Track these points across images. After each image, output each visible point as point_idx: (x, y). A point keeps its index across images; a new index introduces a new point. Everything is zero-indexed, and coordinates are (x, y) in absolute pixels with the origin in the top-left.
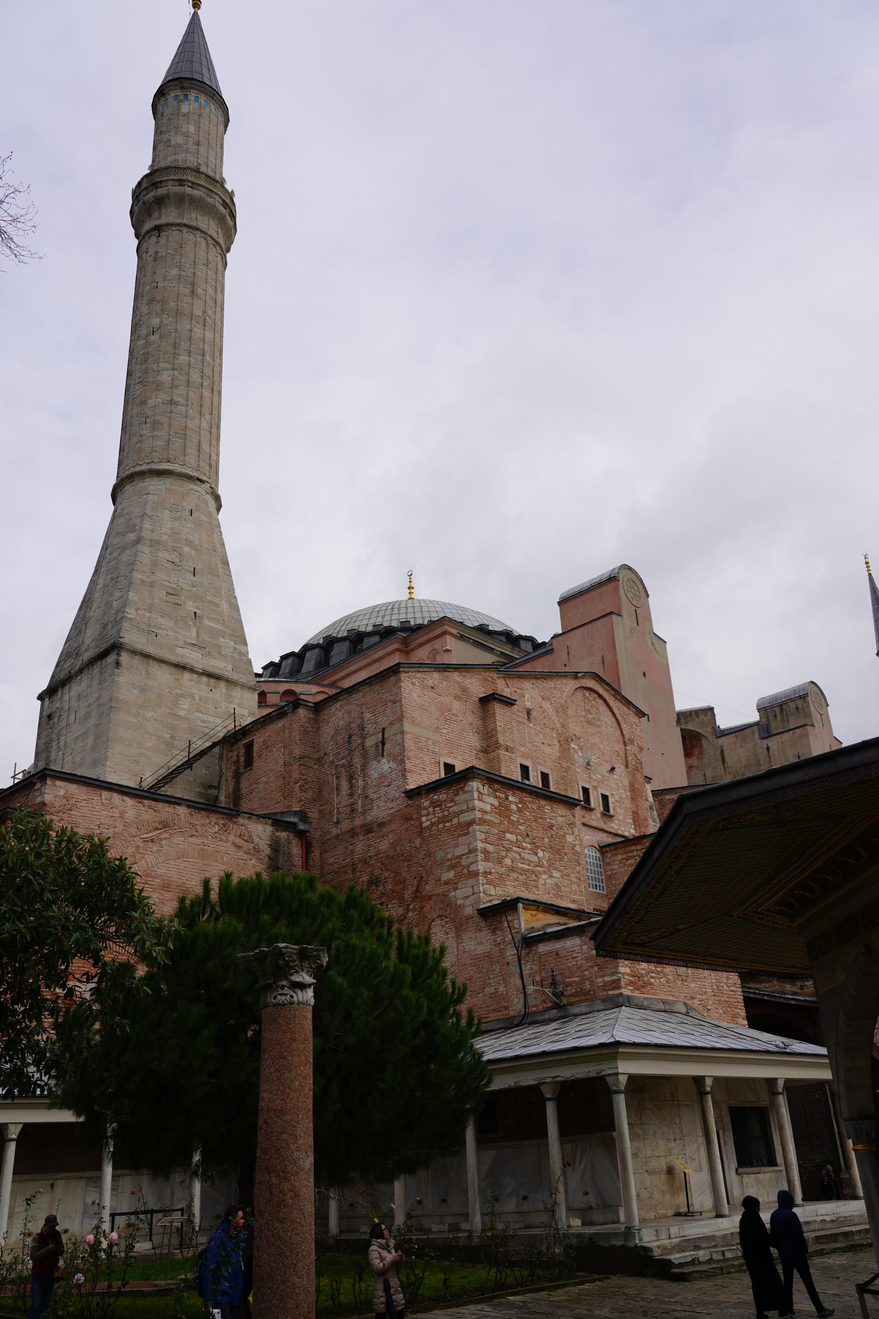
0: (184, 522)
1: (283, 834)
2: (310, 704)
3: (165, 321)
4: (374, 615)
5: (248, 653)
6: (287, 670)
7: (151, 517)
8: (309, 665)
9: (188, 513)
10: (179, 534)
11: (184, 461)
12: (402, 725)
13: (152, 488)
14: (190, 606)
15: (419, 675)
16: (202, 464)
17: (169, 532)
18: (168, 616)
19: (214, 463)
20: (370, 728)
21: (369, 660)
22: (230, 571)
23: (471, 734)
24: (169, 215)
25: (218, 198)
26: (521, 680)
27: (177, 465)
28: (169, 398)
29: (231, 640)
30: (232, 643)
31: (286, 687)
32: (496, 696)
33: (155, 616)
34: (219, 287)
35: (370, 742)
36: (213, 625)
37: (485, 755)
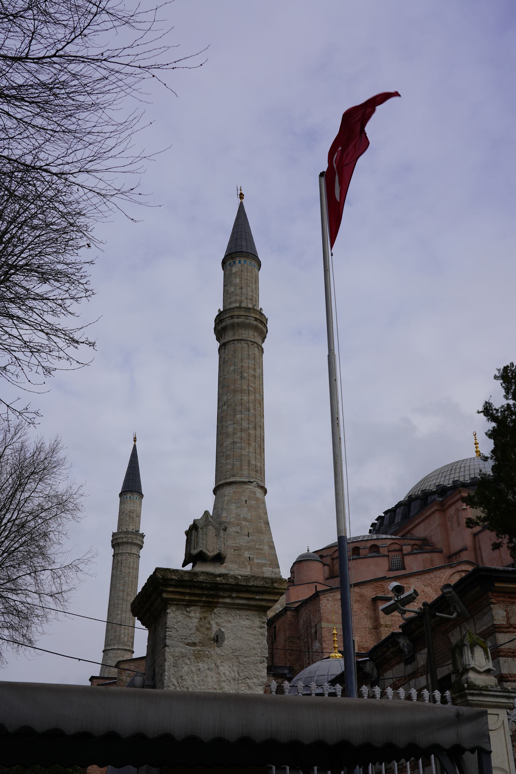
0: (242, 508)
1: (279, 680)
2: (292, 609)
3: (229, 397)
4: (440, 476)
5: (280, 572)
6: (387, 522)
7: (226, 509)
8: (398, 519)
9: (244, 503)
10: (240, 515)
11: (241, 474)
12: (321, 624)
13: (227, 492)
14: (247, 554)
15: (331, 594)
16: (251, 472)
17: (235, 515)
18: (235, 562)
19: (258, 469)
20: (313, 624)
21: (423, 517)
22: (270, 528)
23: (366, 620)
24: (229, 336)
25: (252, 318)
26: (408, 579)
27: (238, 477)
28: (233, 441)
29: (270, 567)
30: (271, 569)
31: (372, 543)
32: (378, 598)
33: (228, 564)
34: (258, 365)
35: (313, 630)
36: (260, 561)
37: (375, 630)
